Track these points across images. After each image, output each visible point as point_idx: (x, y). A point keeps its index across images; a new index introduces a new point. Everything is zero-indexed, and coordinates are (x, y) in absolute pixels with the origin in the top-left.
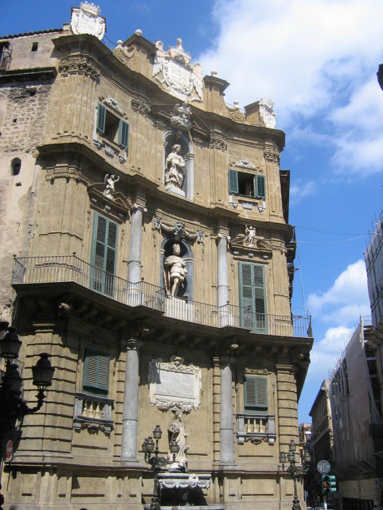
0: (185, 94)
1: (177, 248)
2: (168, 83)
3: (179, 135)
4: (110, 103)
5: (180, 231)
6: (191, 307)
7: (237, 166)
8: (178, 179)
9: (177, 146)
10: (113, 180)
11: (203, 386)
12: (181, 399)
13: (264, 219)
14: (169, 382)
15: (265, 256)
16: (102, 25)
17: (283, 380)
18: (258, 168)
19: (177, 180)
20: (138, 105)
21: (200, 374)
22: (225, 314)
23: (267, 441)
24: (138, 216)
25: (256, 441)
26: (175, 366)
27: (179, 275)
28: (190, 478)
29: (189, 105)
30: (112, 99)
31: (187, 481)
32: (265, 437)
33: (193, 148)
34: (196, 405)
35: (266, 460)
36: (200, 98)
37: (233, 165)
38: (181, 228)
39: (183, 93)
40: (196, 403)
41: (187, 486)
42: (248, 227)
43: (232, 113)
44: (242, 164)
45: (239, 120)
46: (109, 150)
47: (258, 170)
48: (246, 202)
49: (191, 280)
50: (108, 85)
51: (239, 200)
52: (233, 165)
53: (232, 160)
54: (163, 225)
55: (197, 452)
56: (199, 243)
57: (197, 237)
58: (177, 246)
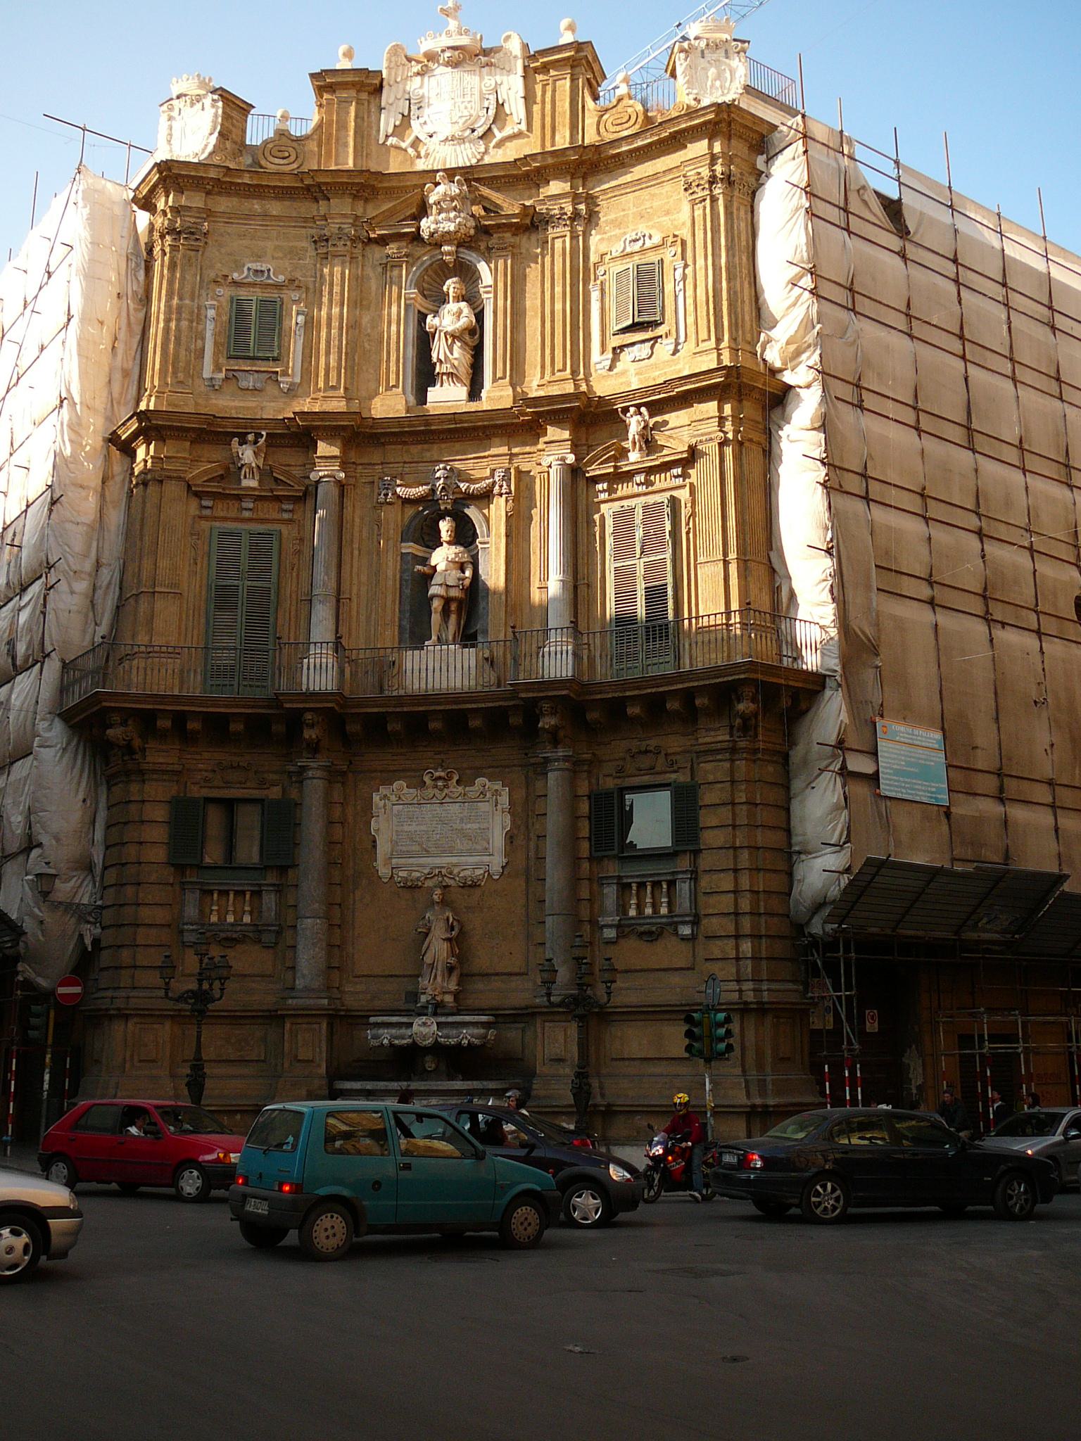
1: (445, 526)
3: (449, 253)
6: (470, 656)
11: (513, 822)
12: (454, 860)
13: (680, 371)
14: (423, 828)
17: (711, 778)
20: (327, 240)
21: (504, 799)
22: (559, 648)
24: (326, 493)
25: (650, 933)
26: (436, 791)
28: (415, 1027)
29: (451, 173)
31: (409, 1032)
32: (670, 924)
34: (496, 868)
35: (676, 979)
40: (497, 862)
43: (605, 117)
46: (249, 382)
48: (633, 344)
50: (242, 236)
51: (614, 349)
53: (603, 249)
56: (501, 495)
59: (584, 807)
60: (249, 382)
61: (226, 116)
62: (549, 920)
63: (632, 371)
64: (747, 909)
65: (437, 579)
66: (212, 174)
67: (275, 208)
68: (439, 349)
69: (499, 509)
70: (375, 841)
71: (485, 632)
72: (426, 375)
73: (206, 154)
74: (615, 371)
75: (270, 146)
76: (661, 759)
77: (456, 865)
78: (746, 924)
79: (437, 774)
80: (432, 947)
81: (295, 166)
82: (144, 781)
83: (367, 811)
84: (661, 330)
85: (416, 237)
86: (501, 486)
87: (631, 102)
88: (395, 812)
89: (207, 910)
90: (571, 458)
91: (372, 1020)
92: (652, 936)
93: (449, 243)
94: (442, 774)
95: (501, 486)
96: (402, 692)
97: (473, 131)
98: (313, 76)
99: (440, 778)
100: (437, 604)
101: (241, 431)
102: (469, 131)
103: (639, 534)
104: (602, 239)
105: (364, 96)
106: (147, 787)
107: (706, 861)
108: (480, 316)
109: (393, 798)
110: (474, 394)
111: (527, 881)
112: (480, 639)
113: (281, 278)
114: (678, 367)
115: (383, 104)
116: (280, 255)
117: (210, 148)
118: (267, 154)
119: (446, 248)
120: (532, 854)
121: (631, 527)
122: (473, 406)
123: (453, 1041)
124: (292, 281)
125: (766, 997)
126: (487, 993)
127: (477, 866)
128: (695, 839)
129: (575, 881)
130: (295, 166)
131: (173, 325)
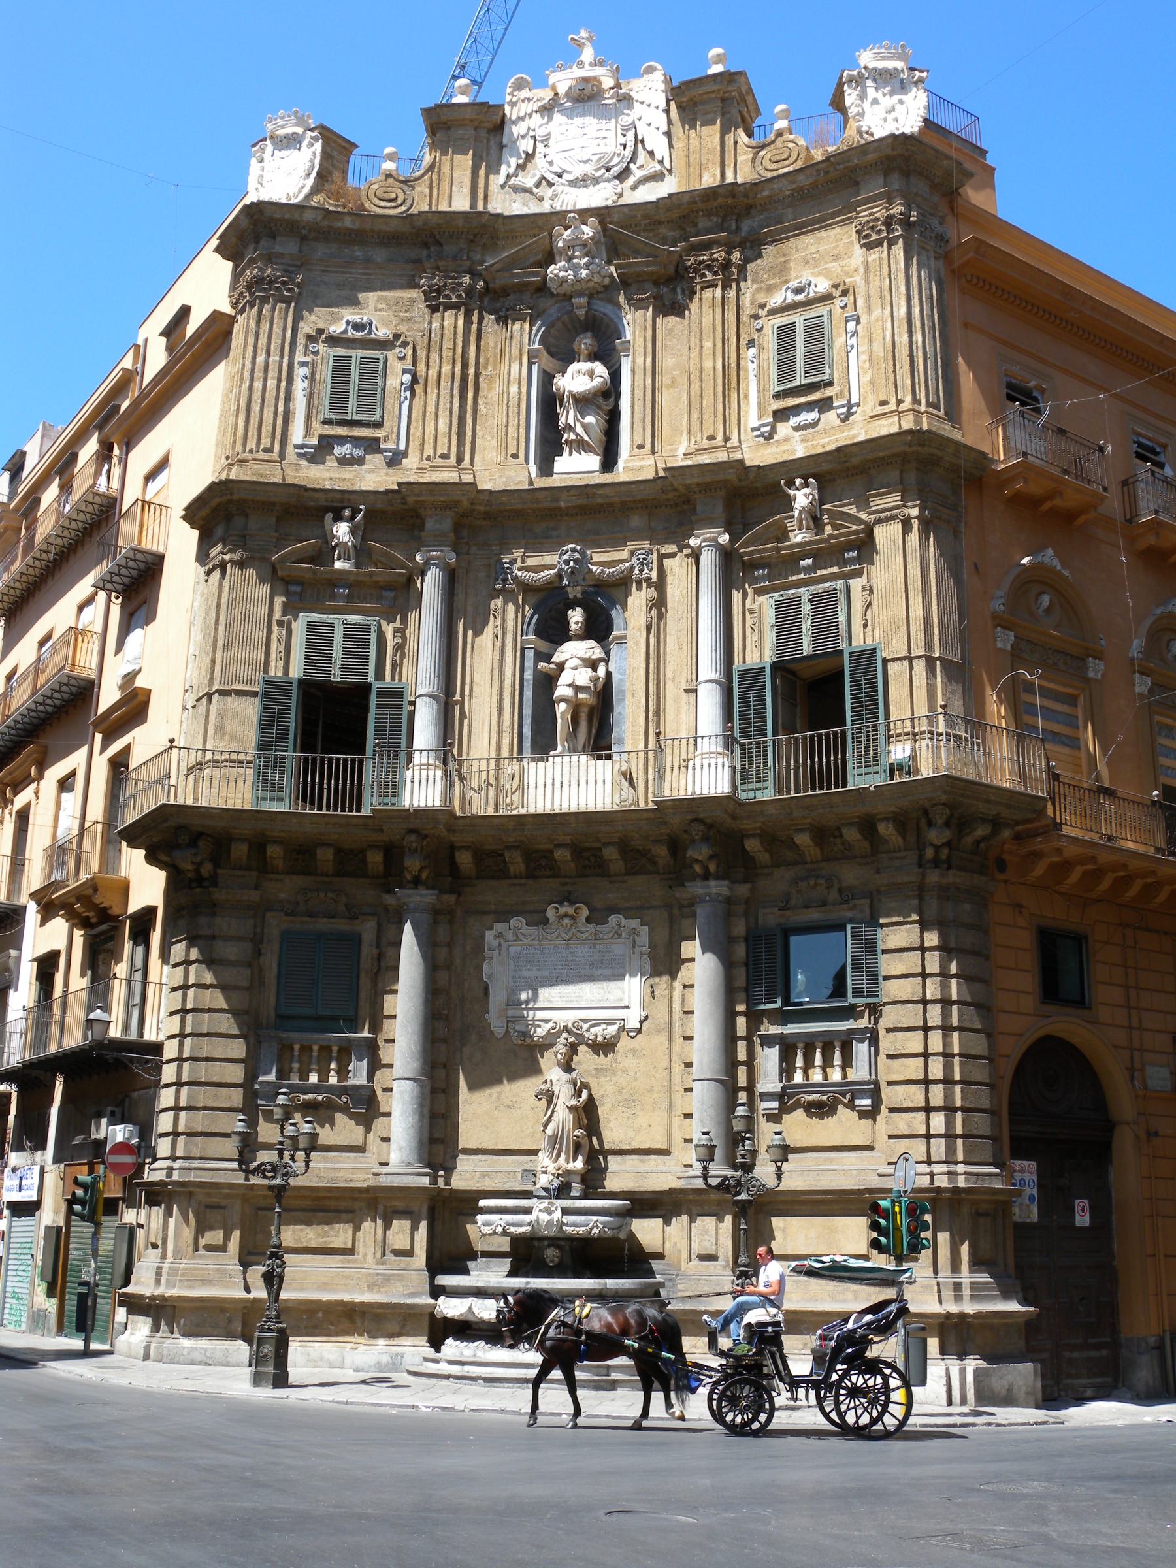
0: (608, 180)
1: (576, 617)
2: (550, 177)
4: (345, 331)
5: (572, 572)
6: (605, 770)
7: (773, 312)
8: (579, 429)
9: (585, 343)
10: (351, 519)
13: (854, 437)
15: (803, 563)
16: (313, 149)
18: (836, 286)
19: (577, 435)
23: (851, 1106)
25: (819, 1105)
27: (569, 692)
28: (535, 1212)
29: (584, 214)
30: (350, 318)
31: (526, 1218)
33: (634, 324)
34: (633, 1023)
36: (661, 162)
37: (763, 313)
38: (572, 563)
39: (596, 181)
41: (529, 1228)
42: (790, 484)
43: (762, 153)
44: (791, 298)
45: (787, 162)
46: (345, 450)
47: (837, 293)
49: (623, 692)
51: (775, 413)
52: (763, 313)
53: (761, 299)
54: (519, 573)
55: (636, 1145)
56: (639, 584)
57: (632, 568)
58: (575, 613)
59: (740, 951)
60: (345, 450)
61: (326, 155)
62: (697, 1086)
63: (797, 439)
64: (940, 1076)
65: (565, 678)
66: (308, 216)
67: (380, 255)
68: (568, 416)
69: (638, 599)
70: (486, 989)
71: (620, 742)
72: (551, 442)
73: (301, 196)
74: (776, 437)
75: (375, 187)
76: (833, 895)
77: (585, 1021)
78: (937, 1095)
79: (562, 910)
80: (555, 1117)
81: (403, 208)
82: (214, 914)
83: (479, 948)
84: (829, 392)
85: (542, 288)
86: (641, 571)
87: (792, 137)
88: (512, 953)
89: (286, 1066)
90: (725, 539)
91: (483, 1203)
92: (821, 1110)
93: (580, 294)
94: (570, 911)
95: (641, 571)
96: (523, 811)
97: (608, 170)
98: (428, 112)
99: (566, 915)
100: (562, 707)
101: (337, 504)
102: (603, 170)
103: (806, 625)
104: (759, 290)
105: (483, 134)
106: (218, 920)
107: (890, 1016)
108: (615, 376)
109: (510, 936)
110: (609, 461)
111: (670, 1040)
112: (615, 748)
113: (383, 332)
114: (851, 433)
115: (505, 141)
116: (384, 306)
117: (307, 190)
118: (371, 196)
119: (577, 301)
120: (677, 1006)
121: (797, 617)
122: (608, 478)
123: (581, 1230)
124: (397, 337)
125: (962, 1182)
126: (622, 1175)
127: (610, 1022)
128: (874, 991)
129: (730, 1038)
130: (403, 208)
131: (258, 384)
